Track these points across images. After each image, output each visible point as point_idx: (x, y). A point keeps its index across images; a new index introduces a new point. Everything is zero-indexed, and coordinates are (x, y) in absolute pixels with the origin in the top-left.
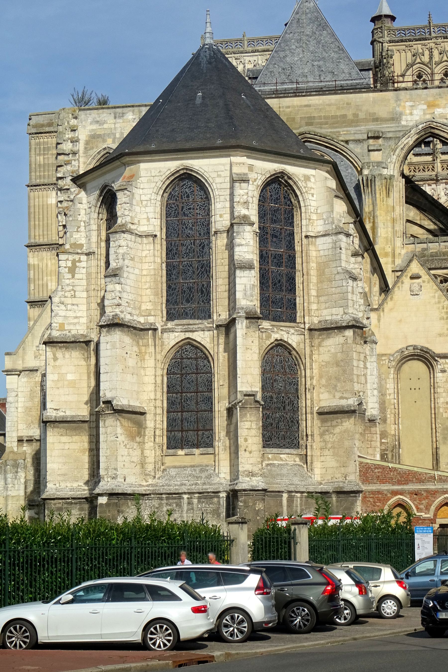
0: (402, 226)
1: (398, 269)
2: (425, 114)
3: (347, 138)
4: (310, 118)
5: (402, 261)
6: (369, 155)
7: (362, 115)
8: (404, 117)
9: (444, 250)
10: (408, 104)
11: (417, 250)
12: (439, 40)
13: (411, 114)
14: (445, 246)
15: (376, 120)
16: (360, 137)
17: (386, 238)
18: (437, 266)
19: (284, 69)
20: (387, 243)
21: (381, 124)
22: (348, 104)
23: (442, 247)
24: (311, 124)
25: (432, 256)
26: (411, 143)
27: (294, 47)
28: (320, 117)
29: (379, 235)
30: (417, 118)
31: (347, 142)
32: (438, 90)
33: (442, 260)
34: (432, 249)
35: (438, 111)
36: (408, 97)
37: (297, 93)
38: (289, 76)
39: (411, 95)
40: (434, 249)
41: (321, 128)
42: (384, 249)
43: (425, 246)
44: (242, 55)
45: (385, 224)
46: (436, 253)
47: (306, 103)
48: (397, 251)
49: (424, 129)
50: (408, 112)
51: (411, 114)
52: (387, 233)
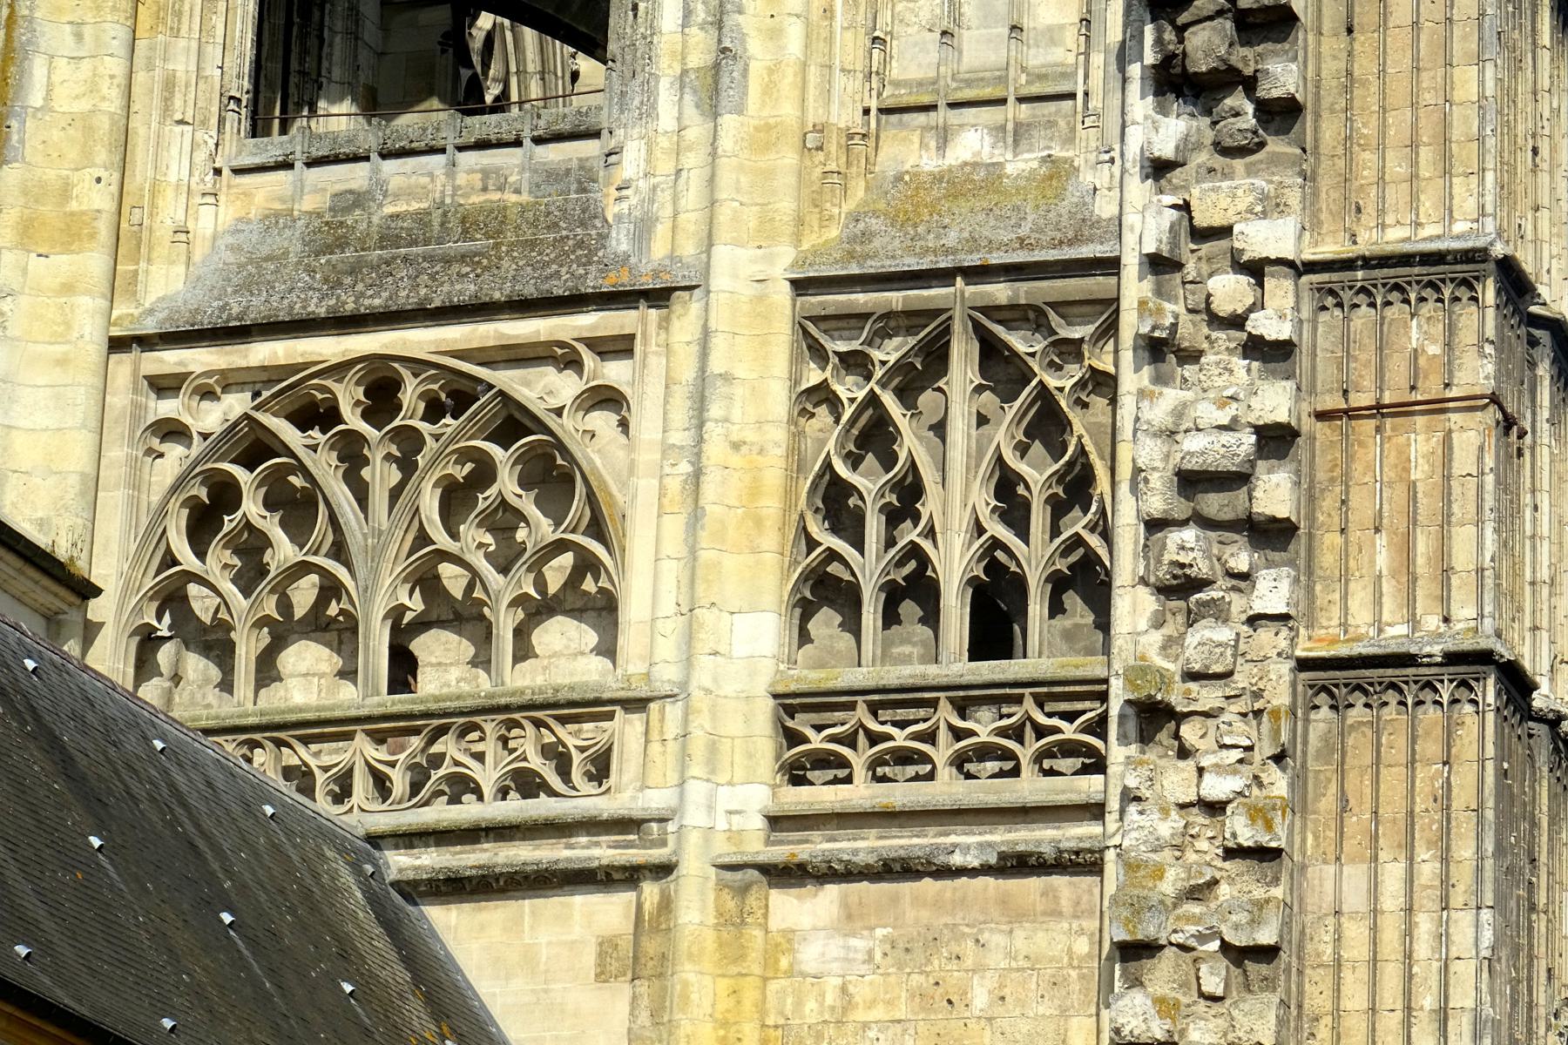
0: (214, 53)
1: (150, 327)
5: (194, 281)
9: (477, 199)
11: (309, 203)
14: (485, 173)
17: (84, 123)
18: (406, 298)
20: (87, 159)
23: (462, 179)
25: (388, 238)
29: (36, 98)
33: (447, 261)
34: (397, 197)
40: (409, 193)
42: (65, 191)
43: (354, 176)
45: (88, 31)
46: (422, 218)
48: (171, 211)
52: (92, 88)
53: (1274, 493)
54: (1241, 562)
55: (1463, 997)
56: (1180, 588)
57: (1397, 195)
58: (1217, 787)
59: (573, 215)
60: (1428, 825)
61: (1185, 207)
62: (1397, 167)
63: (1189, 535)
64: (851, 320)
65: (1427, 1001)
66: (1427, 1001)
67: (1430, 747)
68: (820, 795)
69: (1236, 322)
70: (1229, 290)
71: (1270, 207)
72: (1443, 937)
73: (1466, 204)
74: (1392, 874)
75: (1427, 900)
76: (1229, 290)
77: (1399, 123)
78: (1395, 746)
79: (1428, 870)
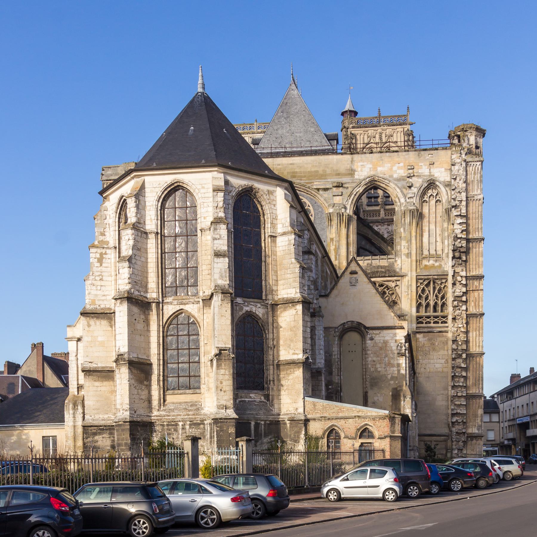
2: (370, 171)
3: (319, 187)
4: (294, 172)
6: (333, 199)
7: (328, 171)
8: (356, 173)
10: (360, 164)
13: (362, 171)
15: (338, 174)
16: (328, 187)
21: (341, 178)
22: (319, 163)
24: (294, 177)
26: (361, 191)
27: (283, 123)
28: (301, 172)
30: (366, 174)
31: (318, 189)
32: (380, 154)
35: (379, 169)
36: (360, 158)
37: (286, 154)
39: (361, 158)
41: (301, 180)
47: (291, 162)
49: (370, 182)
50: (359, 169)
51: (362, 171)
53: (464, 299)
54: (461, 305)
55: (481, 345)
56: (454, 307)
57: (474, 270)
58: (460, 326)
59: (391, 265)
60: (478, 329)
61: (455, 270)
62: (474, 267)
63: (456, 302)
64: (422, 279)
65: (478, 345)
66: (478, 345)
67: (478, 322)
68: (421, 325)
69: (460, 282)
70: (459, 278)
71: (462, 270)
72: (479, 339)
73: (480, 271)
74: (474, 333)
75: (478, 335)
76: (459, 278)
77: (474, 262)
78: (475, 322)
79: (478, 333)
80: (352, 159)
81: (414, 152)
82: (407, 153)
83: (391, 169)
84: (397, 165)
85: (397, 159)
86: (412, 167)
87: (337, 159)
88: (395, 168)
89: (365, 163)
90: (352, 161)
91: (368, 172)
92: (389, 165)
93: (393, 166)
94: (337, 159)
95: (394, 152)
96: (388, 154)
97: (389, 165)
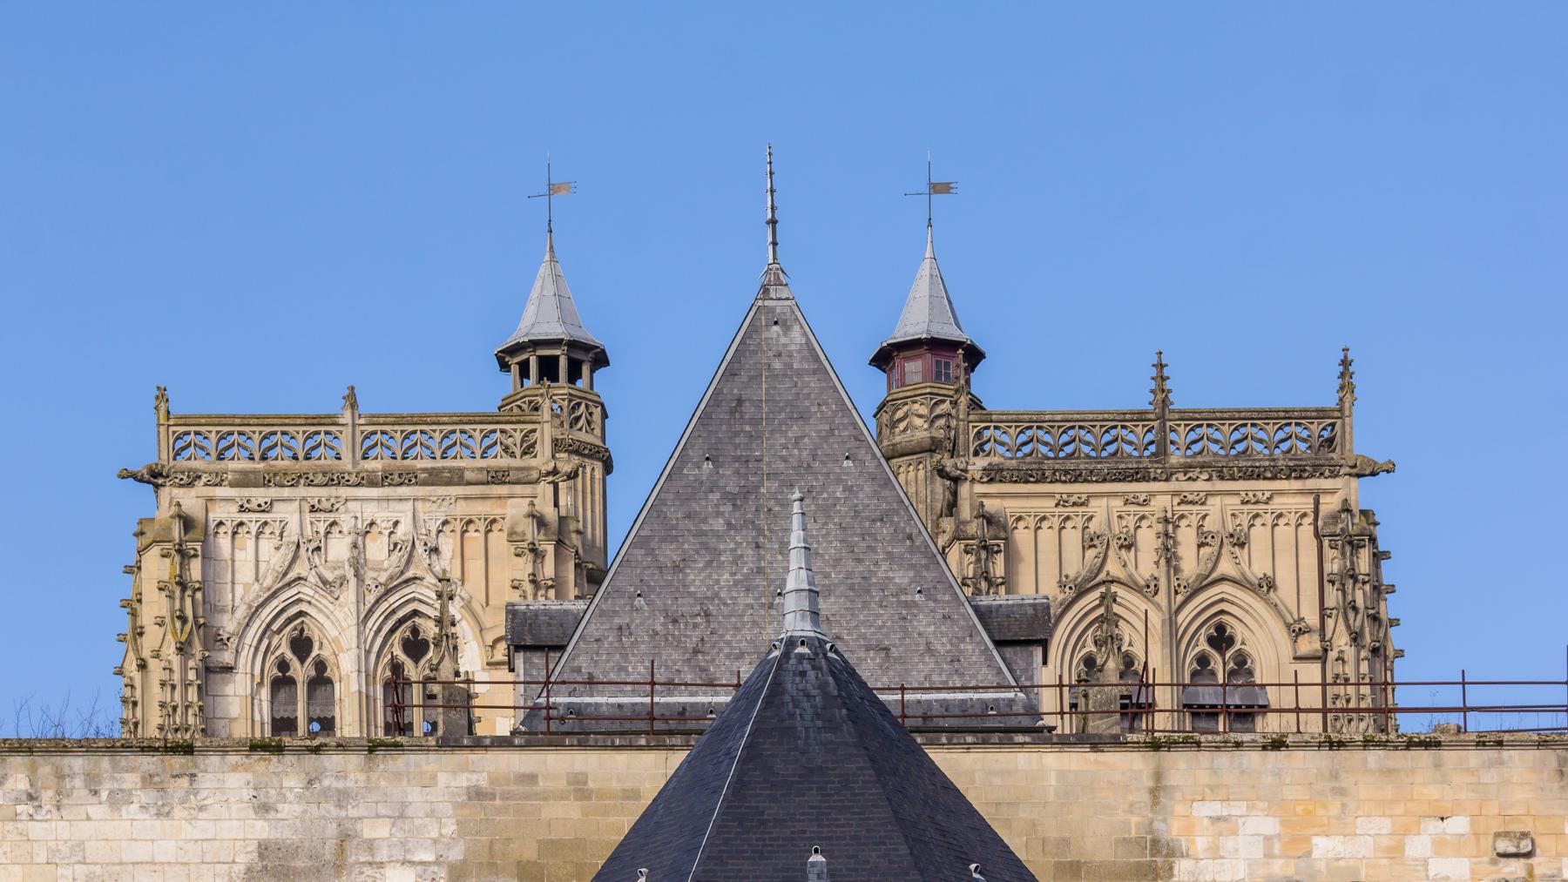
2: (1269, 855)
12: (1201, 485)
13: (1215, 853)
19: (675, 621)
35: (1324, 847)
36: (1204, 777)
38: (696, 652)
39: (1214, 771)
44: (344, 492)
51: (1215, 853)
80: (1158, 776)
81: (1532, 755)
82: (1490, 754)
83: (1395, 852)
84: (1434, 826)
85: (1433, 792)
86: (1525, 846)
87: (1062, 775)
88: (1418, 846)
89: (1238, 809)
90: (1158, 790)
91: (1251, 864)
92: (1385, 825)
93: (1406, 831)
94: (1062, 775)
95: (1410, 744)
96: (1374, 757)
97: (1385, 825)
